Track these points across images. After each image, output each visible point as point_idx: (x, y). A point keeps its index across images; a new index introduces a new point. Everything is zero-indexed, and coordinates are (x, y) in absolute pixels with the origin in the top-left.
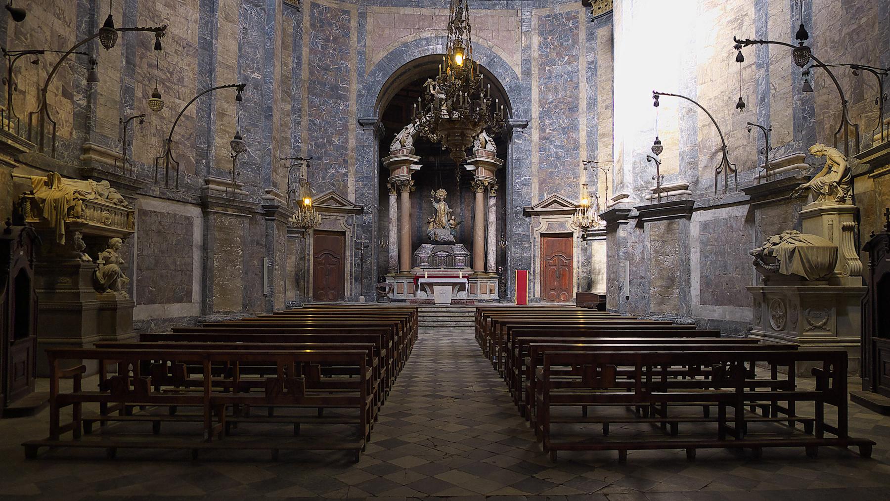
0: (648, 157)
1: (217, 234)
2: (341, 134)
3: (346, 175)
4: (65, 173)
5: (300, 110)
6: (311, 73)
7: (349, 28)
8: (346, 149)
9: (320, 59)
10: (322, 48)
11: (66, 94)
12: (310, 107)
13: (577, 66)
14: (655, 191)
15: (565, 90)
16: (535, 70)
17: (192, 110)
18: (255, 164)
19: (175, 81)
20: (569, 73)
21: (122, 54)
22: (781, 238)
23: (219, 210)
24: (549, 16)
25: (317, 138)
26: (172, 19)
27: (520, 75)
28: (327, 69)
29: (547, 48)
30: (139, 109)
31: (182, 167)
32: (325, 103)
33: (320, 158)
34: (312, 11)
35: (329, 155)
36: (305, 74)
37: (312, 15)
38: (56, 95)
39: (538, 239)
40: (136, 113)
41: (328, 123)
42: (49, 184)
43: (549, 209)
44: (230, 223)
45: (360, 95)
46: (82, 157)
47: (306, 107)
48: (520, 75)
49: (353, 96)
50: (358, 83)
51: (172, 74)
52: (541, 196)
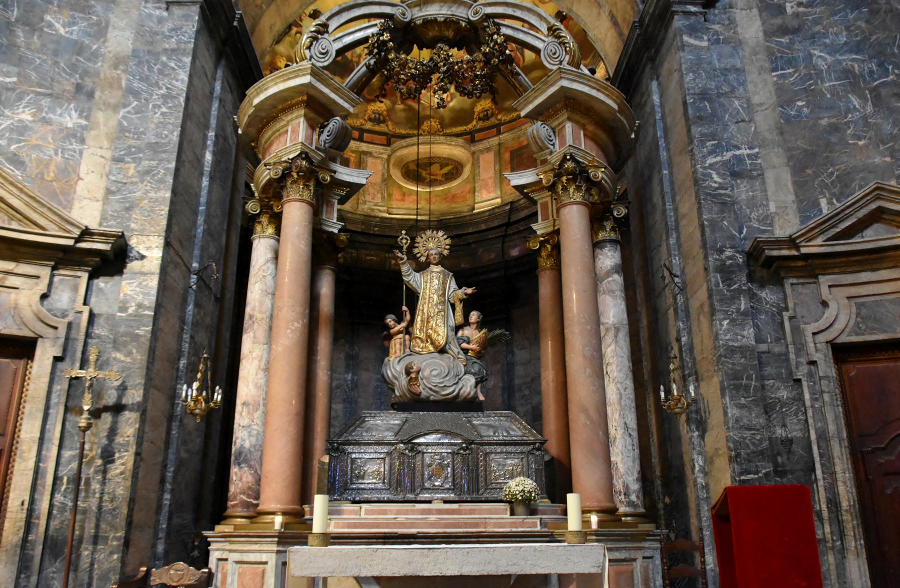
3: (78, 136)
39: (827, 367)
43: (857, 243)
52: (806, 206)
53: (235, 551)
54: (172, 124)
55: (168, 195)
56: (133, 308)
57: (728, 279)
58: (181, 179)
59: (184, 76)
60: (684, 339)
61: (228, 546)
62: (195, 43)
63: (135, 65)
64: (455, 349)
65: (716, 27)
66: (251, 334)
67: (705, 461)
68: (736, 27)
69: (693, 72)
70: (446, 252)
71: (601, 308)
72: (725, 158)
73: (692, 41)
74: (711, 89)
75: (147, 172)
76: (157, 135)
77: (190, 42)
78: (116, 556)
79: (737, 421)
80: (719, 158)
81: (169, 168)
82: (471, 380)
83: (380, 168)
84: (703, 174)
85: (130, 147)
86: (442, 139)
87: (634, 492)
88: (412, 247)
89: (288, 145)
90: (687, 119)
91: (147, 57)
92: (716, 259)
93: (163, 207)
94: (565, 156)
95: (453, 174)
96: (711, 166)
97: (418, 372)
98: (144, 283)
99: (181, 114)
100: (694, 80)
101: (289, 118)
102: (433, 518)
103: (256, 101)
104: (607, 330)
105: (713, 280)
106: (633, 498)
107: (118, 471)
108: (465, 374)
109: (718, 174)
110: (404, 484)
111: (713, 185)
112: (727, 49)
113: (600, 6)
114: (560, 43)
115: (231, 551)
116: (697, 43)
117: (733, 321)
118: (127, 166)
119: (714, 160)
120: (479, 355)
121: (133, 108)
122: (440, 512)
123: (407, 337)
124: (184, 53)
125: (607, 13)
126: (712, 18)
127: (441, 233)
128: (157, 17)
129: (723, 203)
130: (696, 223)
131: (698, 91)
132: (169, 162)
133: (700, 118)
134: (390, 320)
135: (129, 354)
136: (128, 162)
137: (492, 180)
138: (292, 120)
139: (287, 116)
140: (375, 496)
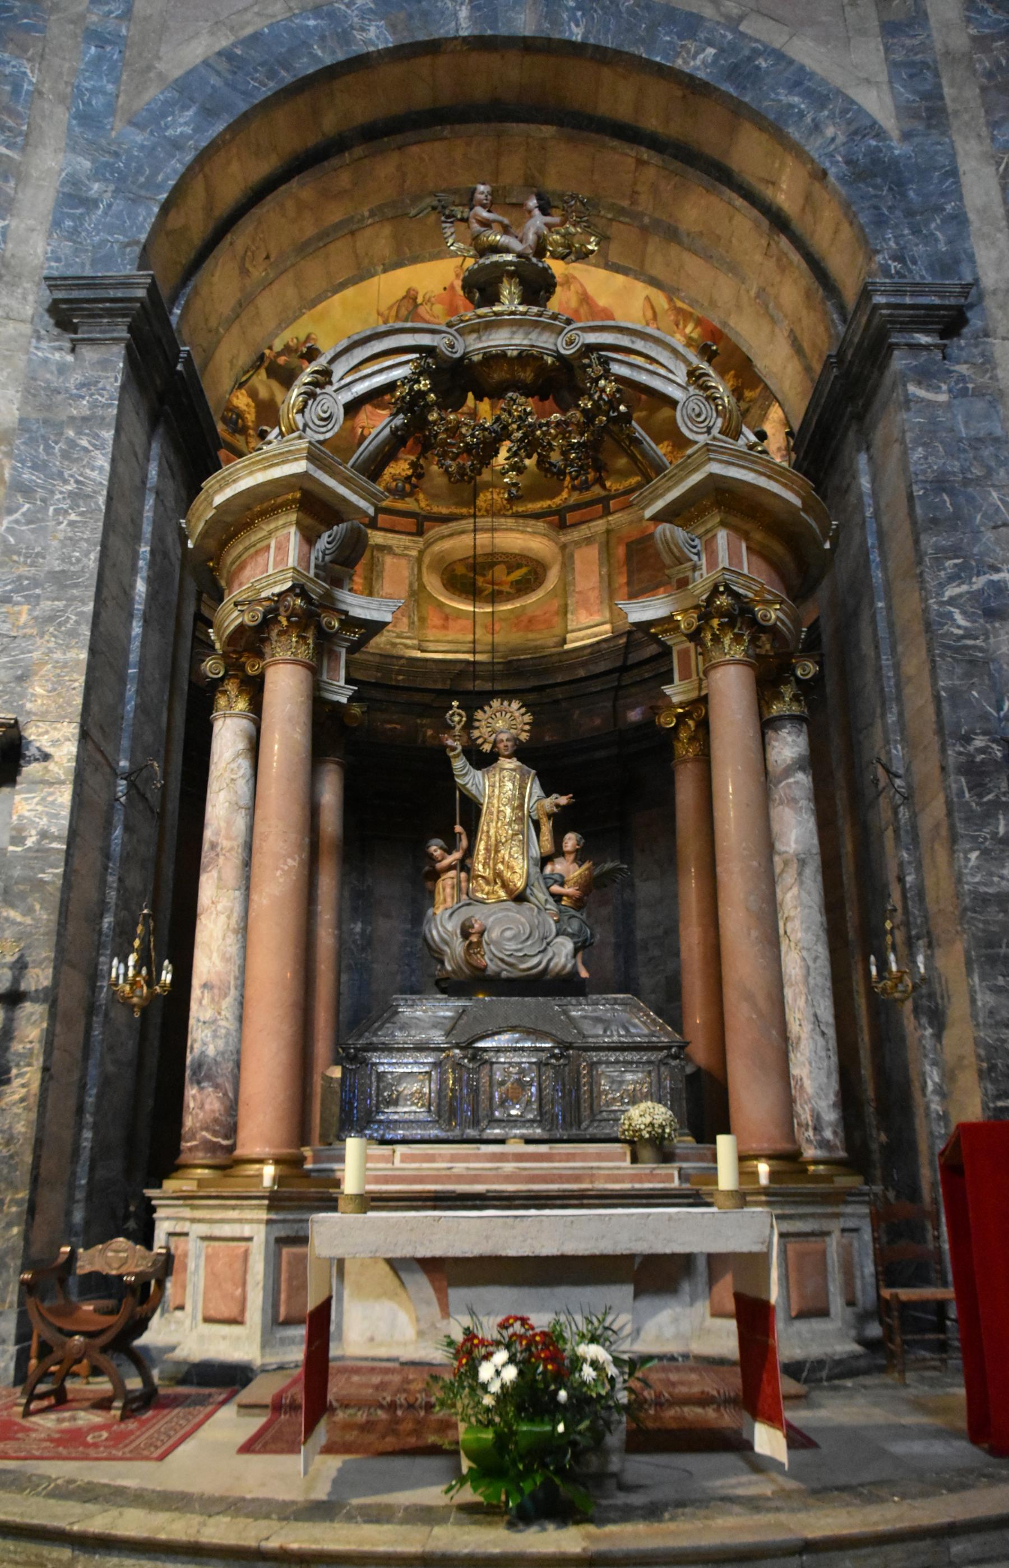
16: (961, 94)
27: (888, 121)
48: (888, 121)
50: (73, 147)
53: (200, 1221)
54: (87, 540)
55: (84, 656)
56: (34, 839)
57: (978, 787)
58: (102, 629)
59: (103, 462)
60: (909, 879)
61: (187, 1213)
62: (119, 406)
63: (24, 443)
64: (540, 895)
65: (963, 369)
66: (214, 874)
67: (943, 1076)
68: (994, 368)
69: (924, 445)
70: (524, 736)
71: (776, 827)
72: (975, 587)
73: (922, 393)
74: (954, 474)
75: (50, 619)
76: (65, 559)
77: (111, 405)
78: (15, 1230)
79: (991, 1013)
80: (964, 588)
81: (82, 613)
82: (567, 945)
83: (406, 573)
84: (940, 615)
85: (20, 578)
86: (510, 522)
87: (830, 1124)
88: (469, 725)
89: (271, 571)
90: (914, 522)
91: (42, 431)
92: (960, 753)
93: (75, 676)
94: (716, 587)
95: (528, 581)
96: (952, 601)
97: (481, 934)
98: (50, 799)
99: (101, 524)
100: (926, 458)
101: (272, 526)
102: (509, 1167)
103: (219, 499)
104: (786, 863)
105: (954, 786)
106: (828, 1134)
107: (17, 1097)
108: (557, 935)
109: (964, 613)
110: (462, 1112)
111: (956, 631)
112: (980, 406)
113: (773, 321)
114: (707, 398)
115: (193, 1220)
116: (930, 396)
117: (985, 853)
118: (16, 608)
119: (958, 590)
120: (579, 904)
121: (24, 514)
122: (519, 1157)
123: (463, 875)
124: (102, 422)
125: (786, 334)
126: (956, 352)
127: (515, 705)
128: (58, 363)
129: (970, 662)
130: (928, 693)
131: (931, 476)
132: (84, 603)
133: (935, 521)
134: (435, 848)
135: (29, 911)
136: (18, 603)
137: (596, 593)
138: (277, 529)
139: (268, 523)
140: (418, 1133)
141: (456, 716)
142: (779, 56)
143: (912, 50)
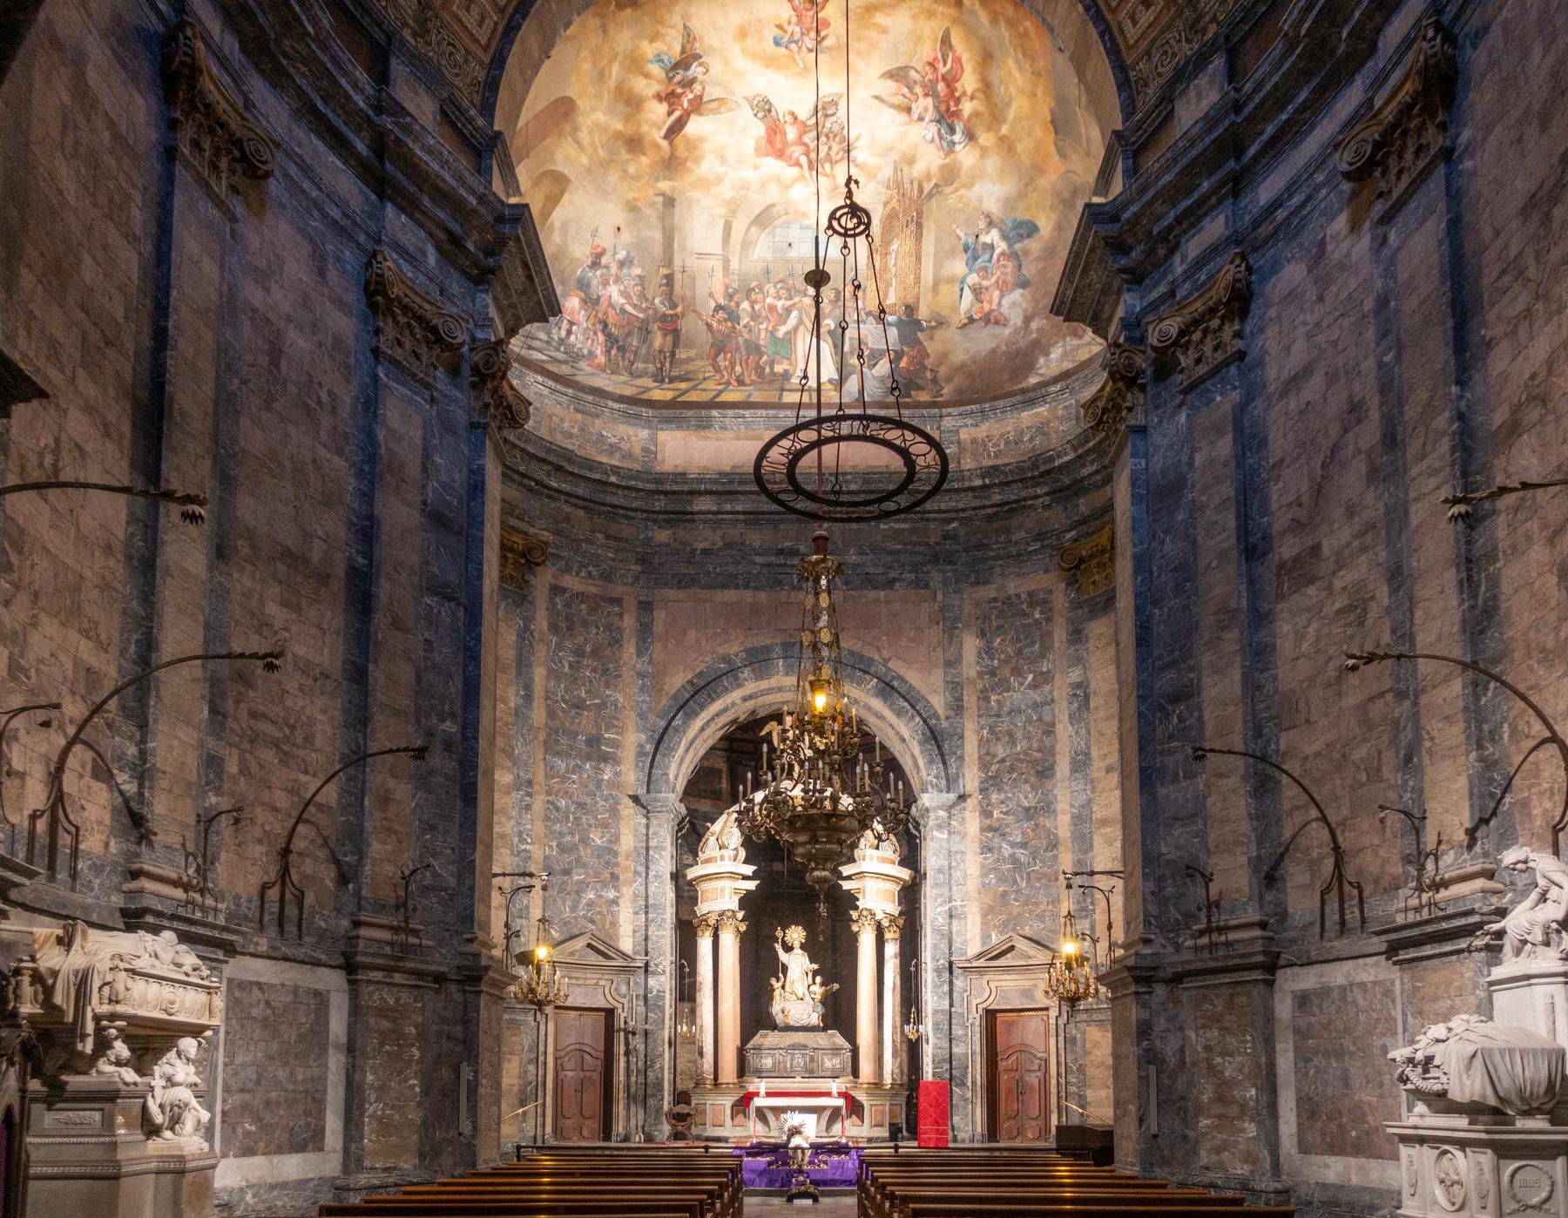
0: (1188, 867)
1: (372, 1021)
2: (606, 826)
3: (615, 902)
4: (94, 918)
5: (530, 783)
6: (551, 714)
7: (619, 630)
8: (616, 854)
9: (567, 690)
10: (571, 667)
11: (102, 773)
12: (548, 777)
13: (1051, 692)
14: (1202, 933)
15: (1028, 737)
16: (970, 700)
17: (331, 795)
18: (445, 890)
19: (299, 740)
20: (1035, 706)
21: (203, 697)
22: (1450, 1030)
23: (377, 975)
24: (995, 600)
25: (561, 834)
26: (294, 628)
28: (579, 706)
29: (992, 658)
30: (232, 794)
31: (309, 899)
32: (578, 769)
33: (567, 872)
34: (551, 600)
35: (585, 866)
36: (538, 715)
37: (553, 611)
38: (81, 776)
40: (225, 803)
41: (582, 806)
42: (65, 942)
44: (397, 1000)
45: (641, 753)
46: (127, 886)
47: (540, 777)
48: (941, 712)
49: (628, 755)
51: (292, 728)
52: (985, 937)
64: (808, 998)
134: (773, 981)
141: (779, 933)
142: (903, 680)
143: (955, 676)
